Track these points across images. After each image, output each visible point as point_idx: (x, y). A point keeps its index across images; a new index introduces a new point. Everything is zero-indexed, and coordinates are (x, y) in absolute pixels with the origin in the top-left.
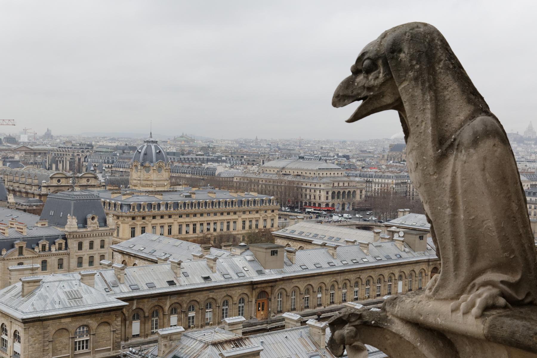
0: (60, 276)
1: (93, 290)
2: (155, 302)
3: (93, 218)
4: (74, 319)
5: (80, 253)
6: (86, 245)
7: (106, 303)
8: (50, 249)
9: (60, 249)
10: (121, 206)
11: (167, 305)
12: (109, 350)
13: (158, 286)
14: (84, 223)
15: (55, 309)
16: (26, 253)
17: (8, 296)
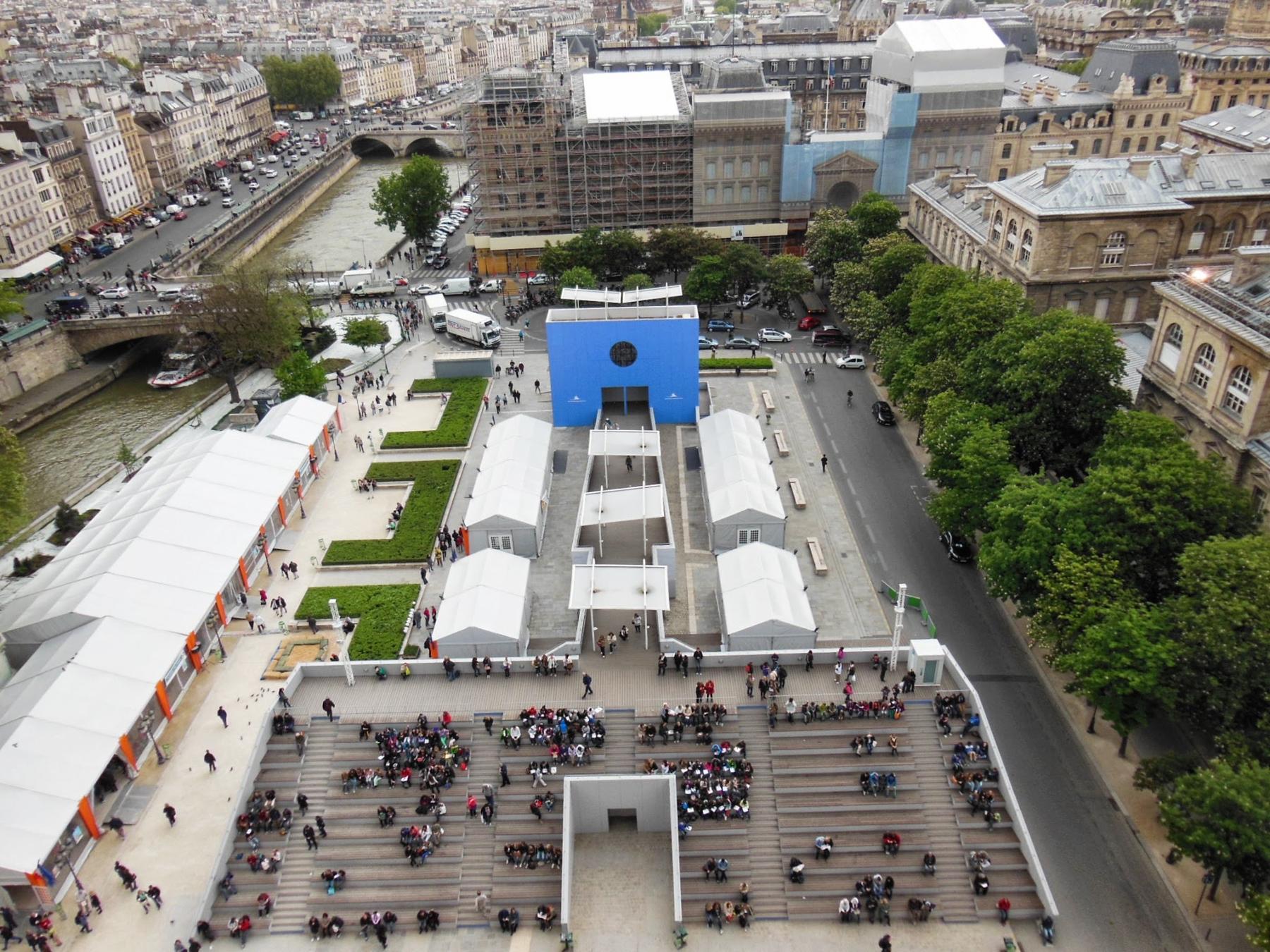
0: (1097, 163)
1: (1142, 185)
2: (1234, 207)
3: (1159, 81)
4: (1108, 222)
5: (1129, 132)
6: (1140, 119)
7: (1160, 203)
8: (1086, 126)
9: (1101, 124)
10: (1206, 61)
11: (1253, 214)
12: (1149, 268)
13: (1245, 186)
14: (1143, 87)
15: (1084, 207)
16: (1052, 130)
17: (1024, 185)
